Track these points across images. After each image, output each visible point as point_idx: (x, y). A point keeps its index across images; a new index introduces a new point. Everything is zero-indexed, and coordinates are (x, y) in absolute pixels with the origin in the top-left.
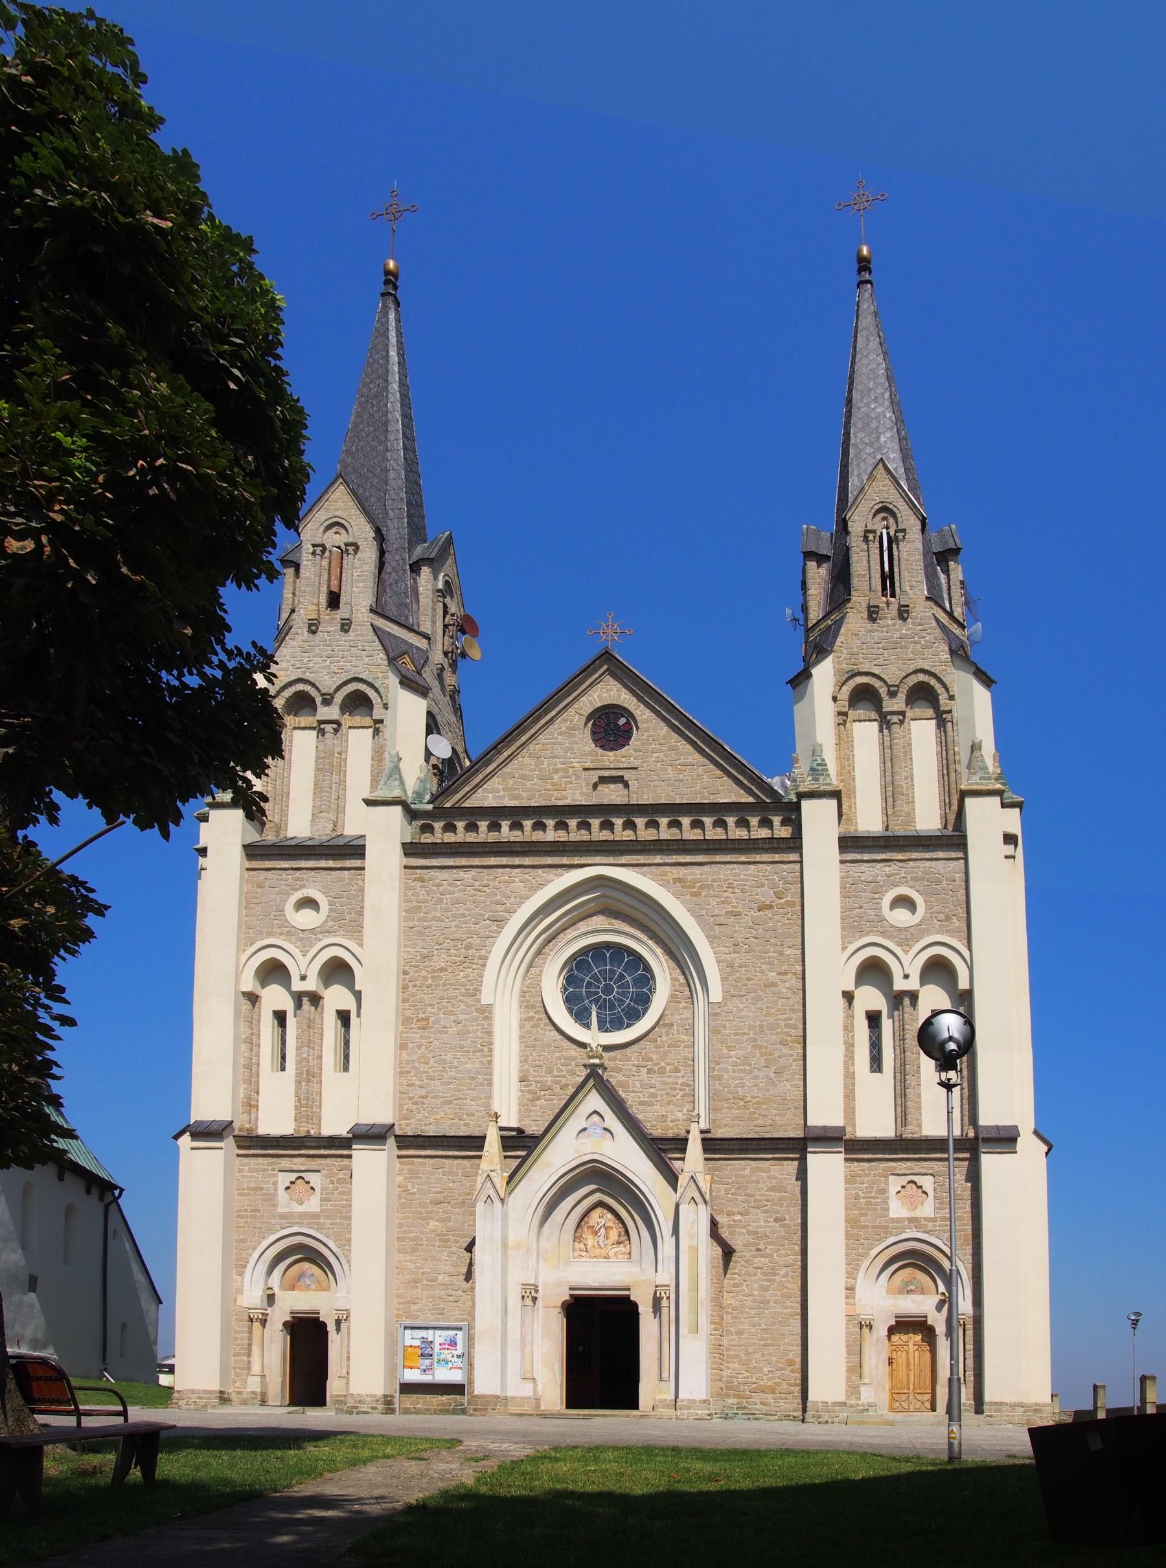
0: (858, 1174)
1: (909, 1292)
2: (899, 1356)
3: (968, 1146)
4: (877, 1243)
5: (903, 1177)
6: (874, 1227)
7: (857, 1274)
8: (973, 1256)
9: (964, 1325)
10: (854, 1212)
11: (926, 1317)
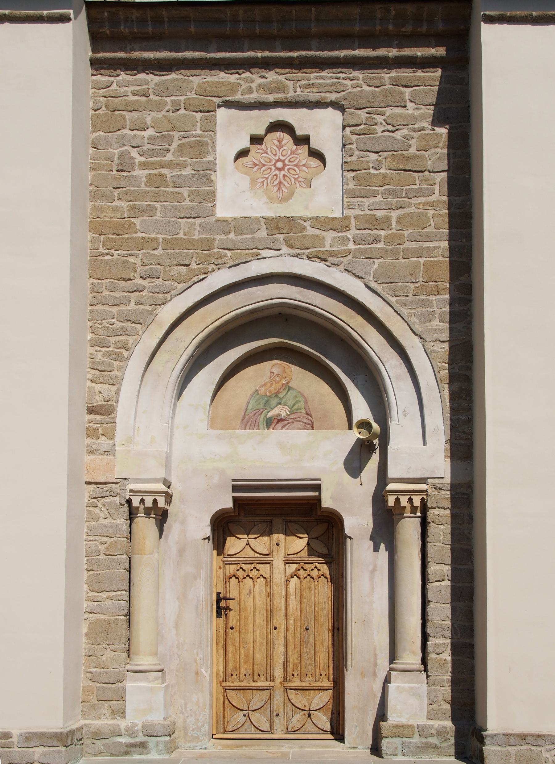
0: (128, 103)
1: (271, 423)
2: (245, 591)
3: (440, 26)
4: (180, 287)
5: (256, 112)
6: (169, 244)
7: (122, 369)
8: (451, 322)
9: (424, 507)
10: (117, 203)
11: (318, 488)
